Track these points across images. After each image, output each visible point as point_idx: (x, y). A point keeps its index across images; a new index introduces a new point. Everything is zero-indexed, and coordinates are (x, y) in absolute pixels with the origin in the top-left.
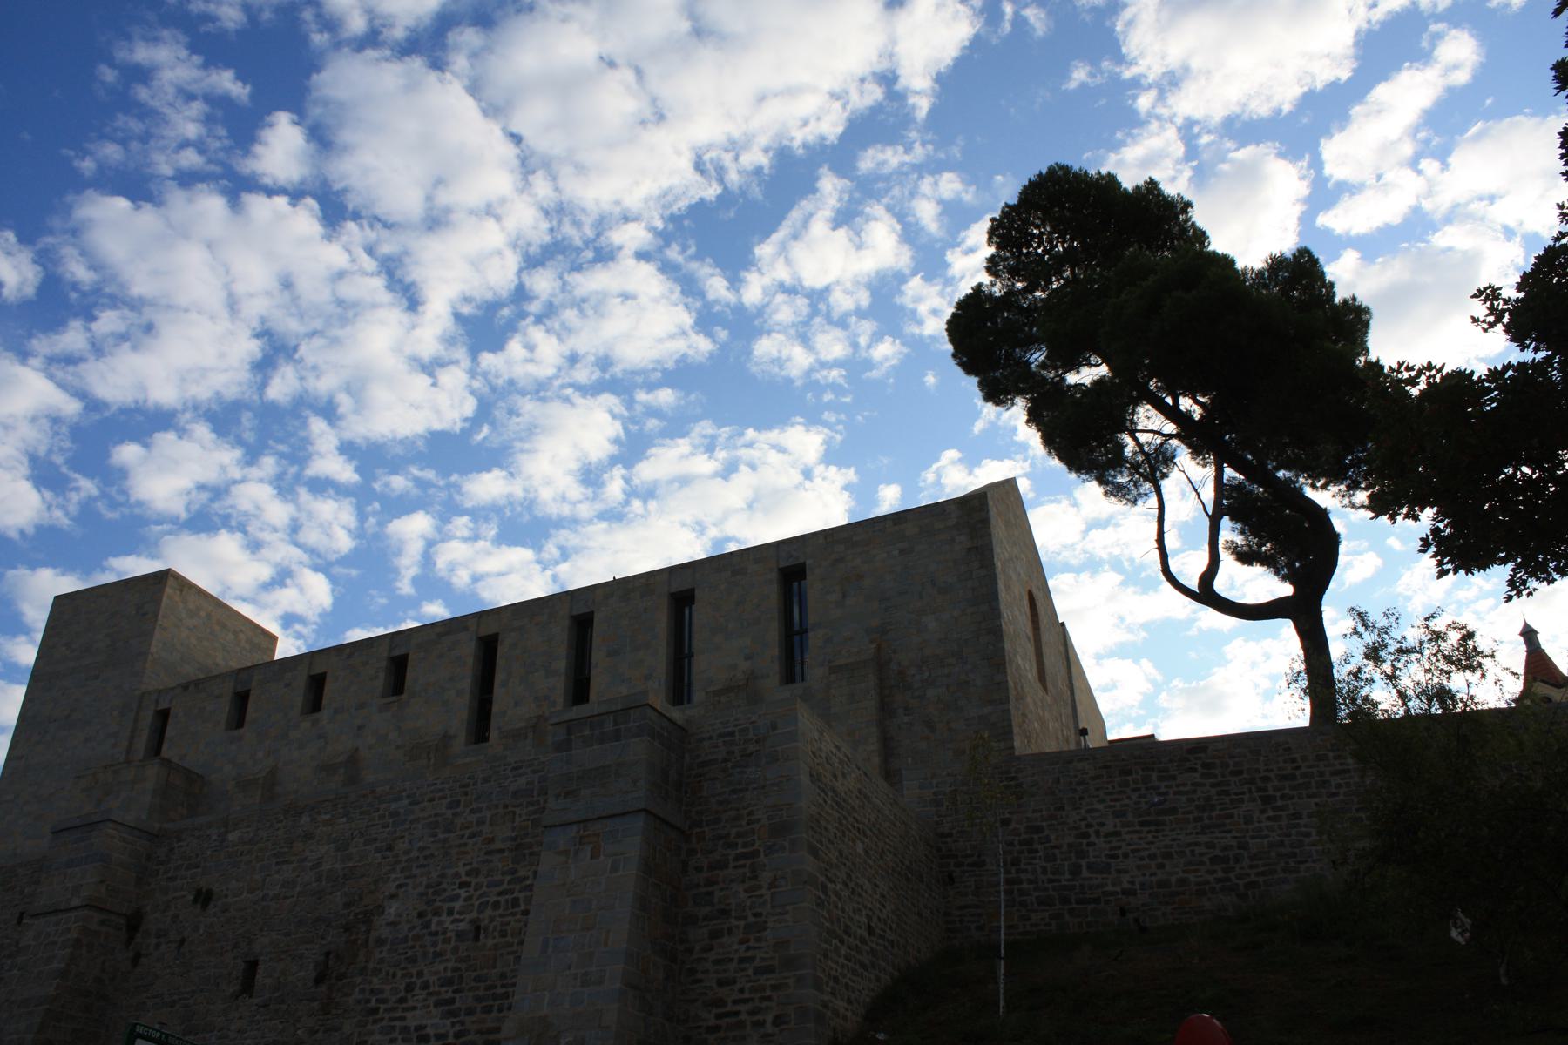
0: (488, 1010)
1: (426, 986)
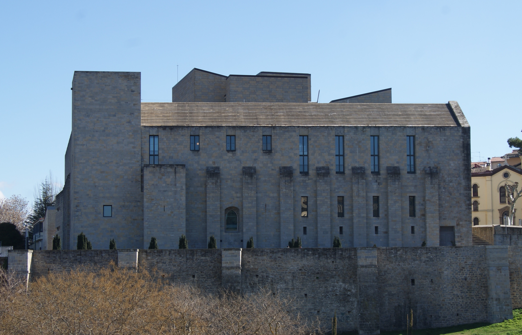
0: (470, 292)
1: (456, 287)
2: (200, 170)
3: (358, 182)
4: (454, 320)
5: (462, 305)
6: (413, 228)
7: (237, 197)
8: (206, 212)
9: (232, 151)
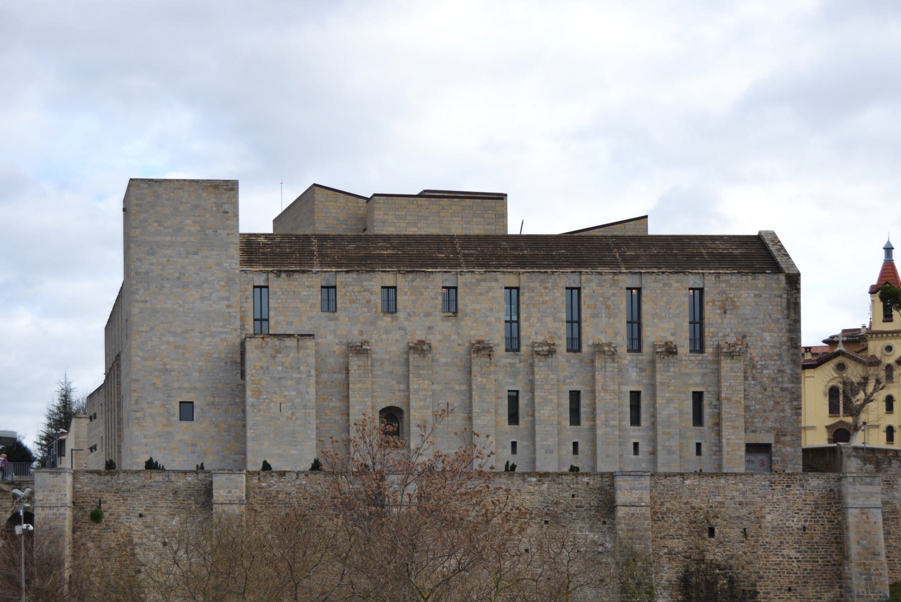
1: (788, 543)
2: (338, 344)
3: (605, 367)
4: (783, 598)
5: (797, 573)
6: (699, 446)
7: (400, 391)
8: (348, 415)
9: (392, 313)
